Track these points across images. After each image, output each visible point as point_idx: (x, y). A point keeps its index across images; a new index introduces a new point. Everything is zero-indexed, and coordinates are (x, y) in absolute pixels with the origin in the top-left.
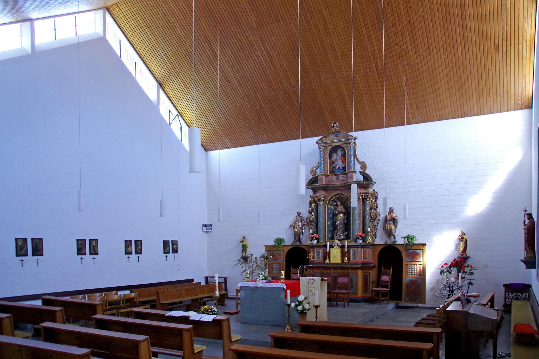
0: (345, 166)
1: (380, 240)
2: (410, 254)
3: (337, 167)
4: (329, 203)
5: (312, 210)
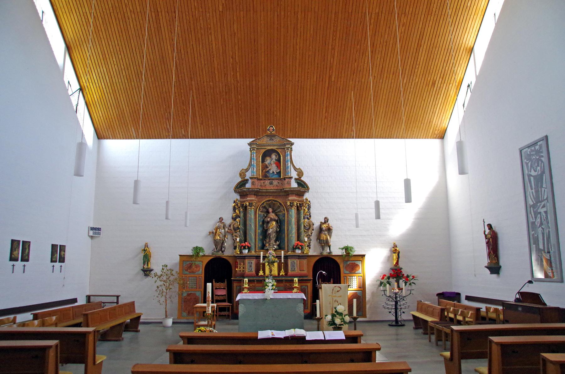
0: (280, 172)
1: (313, 251)
3: (271, 172)
4: (259, 209)
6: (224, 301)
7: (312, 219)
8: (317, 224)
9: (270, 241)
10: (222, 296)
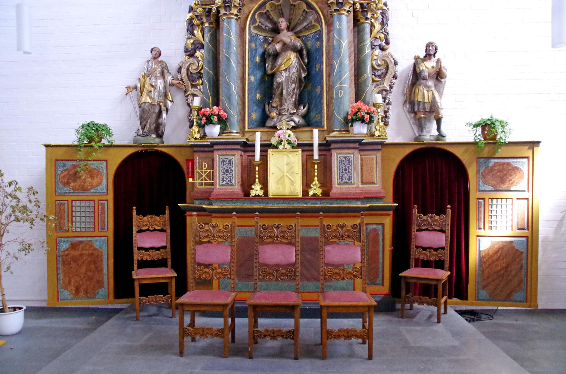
1: (397, 130)
2: (492, 169)
4: (253, 21)
5: (198, 46)
7: (391, 49)
8: (404, 65)
9: (281, 105)
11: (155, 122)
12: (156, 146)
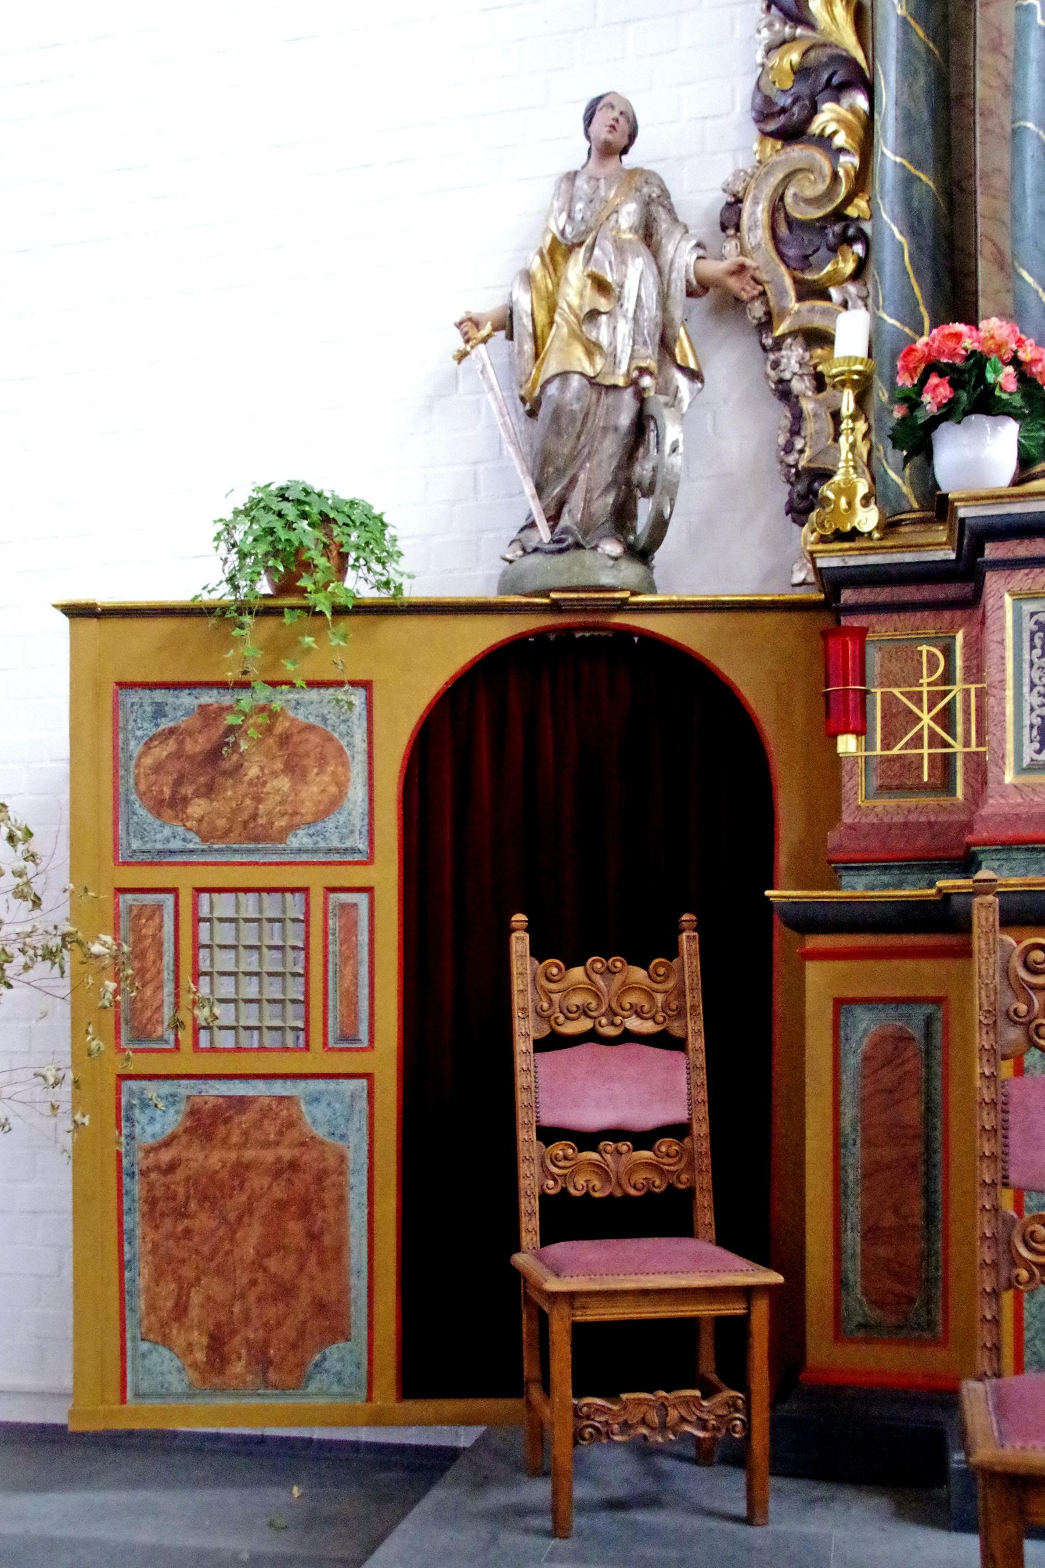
6: (658, 1215)
10: (643, 1139)
11: (615, 483)
12: (623, 606)
